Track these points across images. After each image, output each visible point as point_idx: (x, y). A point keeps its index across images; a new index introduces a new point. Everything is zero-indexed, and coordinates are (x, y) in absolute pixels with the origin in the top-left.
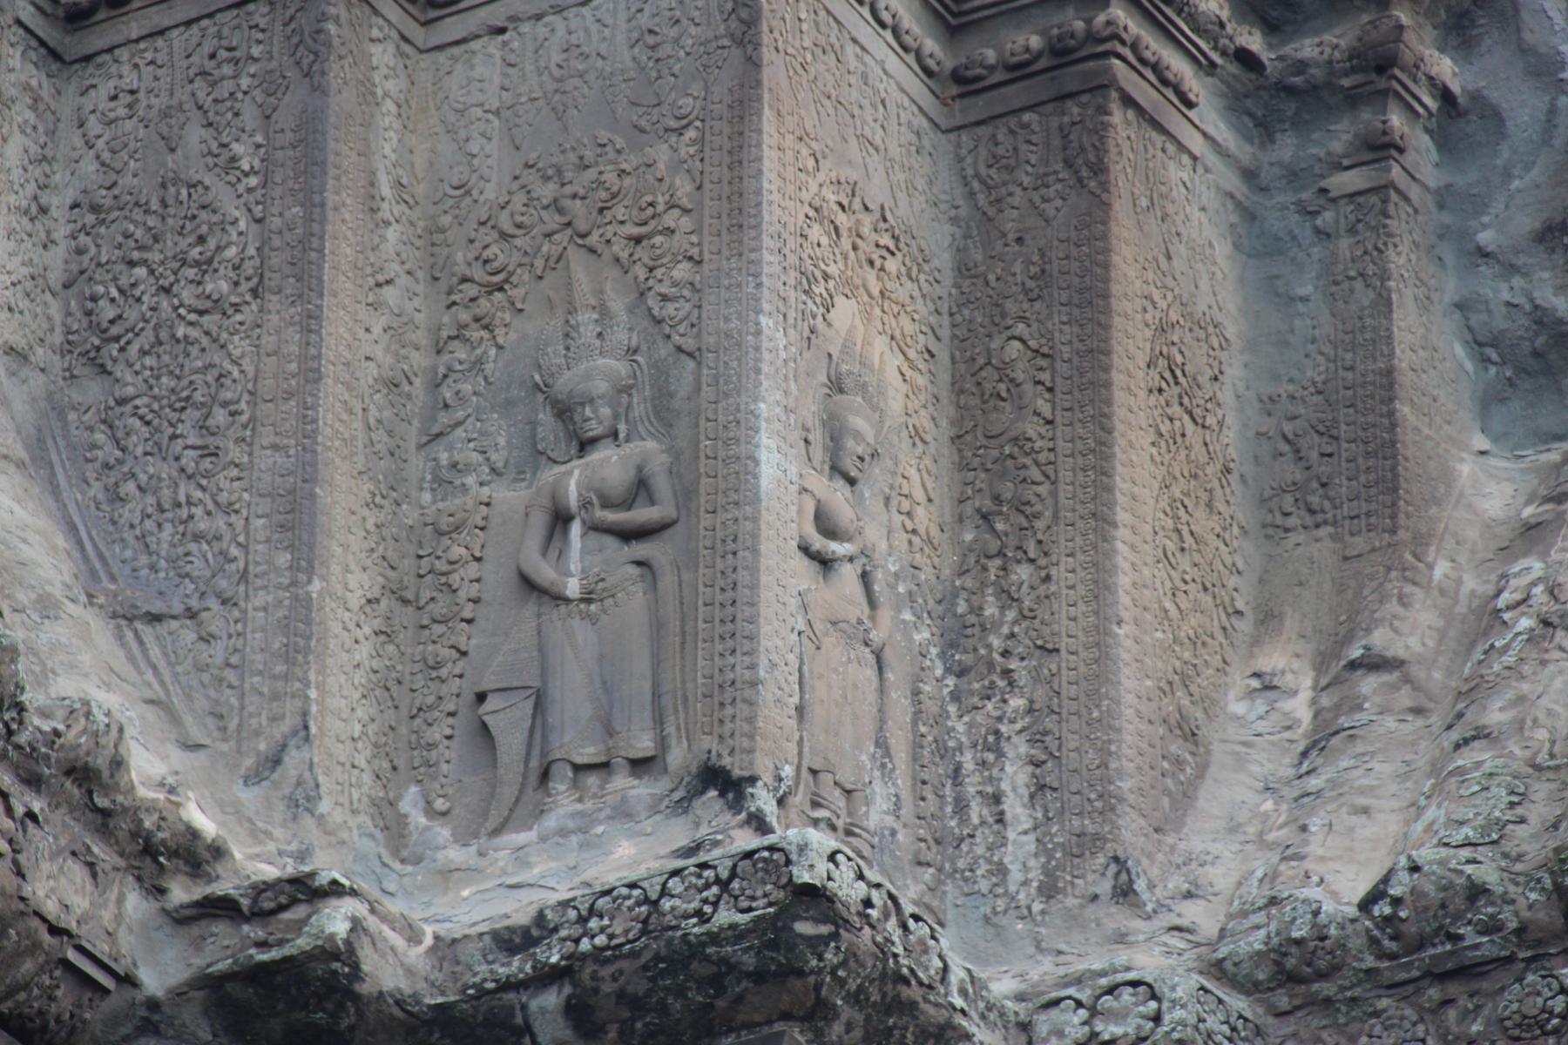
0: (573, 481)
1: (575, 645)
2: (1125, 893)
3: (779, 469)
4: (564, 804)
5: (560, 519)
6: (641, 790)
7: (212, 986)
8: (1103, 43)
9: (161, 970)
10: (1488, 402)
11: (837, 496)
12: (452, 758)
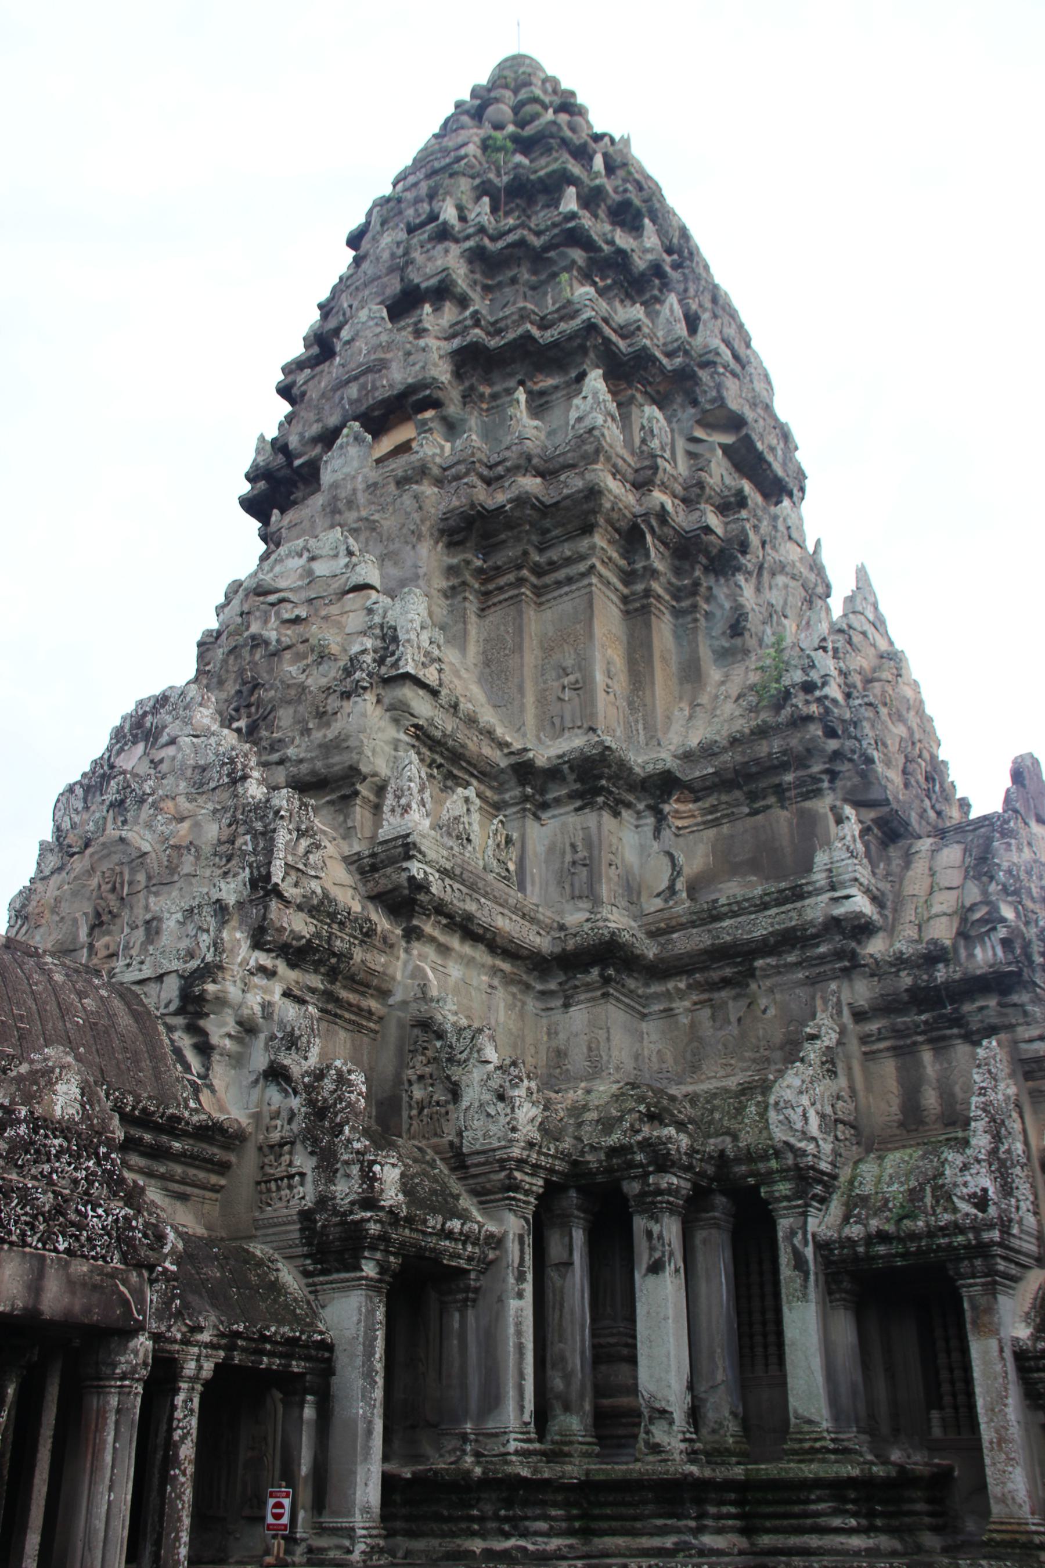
0: (566, 681)
1: (568, 707)
2: (659, 744)
3: (600, 677)
4: (567, 734)
5: (564, 687)
6: (579, 731)
7: (512, 766)
8: (649, 605)
9: (503, 763)
10: (715, 661)
11: (610, 682)
12: (548, 727)
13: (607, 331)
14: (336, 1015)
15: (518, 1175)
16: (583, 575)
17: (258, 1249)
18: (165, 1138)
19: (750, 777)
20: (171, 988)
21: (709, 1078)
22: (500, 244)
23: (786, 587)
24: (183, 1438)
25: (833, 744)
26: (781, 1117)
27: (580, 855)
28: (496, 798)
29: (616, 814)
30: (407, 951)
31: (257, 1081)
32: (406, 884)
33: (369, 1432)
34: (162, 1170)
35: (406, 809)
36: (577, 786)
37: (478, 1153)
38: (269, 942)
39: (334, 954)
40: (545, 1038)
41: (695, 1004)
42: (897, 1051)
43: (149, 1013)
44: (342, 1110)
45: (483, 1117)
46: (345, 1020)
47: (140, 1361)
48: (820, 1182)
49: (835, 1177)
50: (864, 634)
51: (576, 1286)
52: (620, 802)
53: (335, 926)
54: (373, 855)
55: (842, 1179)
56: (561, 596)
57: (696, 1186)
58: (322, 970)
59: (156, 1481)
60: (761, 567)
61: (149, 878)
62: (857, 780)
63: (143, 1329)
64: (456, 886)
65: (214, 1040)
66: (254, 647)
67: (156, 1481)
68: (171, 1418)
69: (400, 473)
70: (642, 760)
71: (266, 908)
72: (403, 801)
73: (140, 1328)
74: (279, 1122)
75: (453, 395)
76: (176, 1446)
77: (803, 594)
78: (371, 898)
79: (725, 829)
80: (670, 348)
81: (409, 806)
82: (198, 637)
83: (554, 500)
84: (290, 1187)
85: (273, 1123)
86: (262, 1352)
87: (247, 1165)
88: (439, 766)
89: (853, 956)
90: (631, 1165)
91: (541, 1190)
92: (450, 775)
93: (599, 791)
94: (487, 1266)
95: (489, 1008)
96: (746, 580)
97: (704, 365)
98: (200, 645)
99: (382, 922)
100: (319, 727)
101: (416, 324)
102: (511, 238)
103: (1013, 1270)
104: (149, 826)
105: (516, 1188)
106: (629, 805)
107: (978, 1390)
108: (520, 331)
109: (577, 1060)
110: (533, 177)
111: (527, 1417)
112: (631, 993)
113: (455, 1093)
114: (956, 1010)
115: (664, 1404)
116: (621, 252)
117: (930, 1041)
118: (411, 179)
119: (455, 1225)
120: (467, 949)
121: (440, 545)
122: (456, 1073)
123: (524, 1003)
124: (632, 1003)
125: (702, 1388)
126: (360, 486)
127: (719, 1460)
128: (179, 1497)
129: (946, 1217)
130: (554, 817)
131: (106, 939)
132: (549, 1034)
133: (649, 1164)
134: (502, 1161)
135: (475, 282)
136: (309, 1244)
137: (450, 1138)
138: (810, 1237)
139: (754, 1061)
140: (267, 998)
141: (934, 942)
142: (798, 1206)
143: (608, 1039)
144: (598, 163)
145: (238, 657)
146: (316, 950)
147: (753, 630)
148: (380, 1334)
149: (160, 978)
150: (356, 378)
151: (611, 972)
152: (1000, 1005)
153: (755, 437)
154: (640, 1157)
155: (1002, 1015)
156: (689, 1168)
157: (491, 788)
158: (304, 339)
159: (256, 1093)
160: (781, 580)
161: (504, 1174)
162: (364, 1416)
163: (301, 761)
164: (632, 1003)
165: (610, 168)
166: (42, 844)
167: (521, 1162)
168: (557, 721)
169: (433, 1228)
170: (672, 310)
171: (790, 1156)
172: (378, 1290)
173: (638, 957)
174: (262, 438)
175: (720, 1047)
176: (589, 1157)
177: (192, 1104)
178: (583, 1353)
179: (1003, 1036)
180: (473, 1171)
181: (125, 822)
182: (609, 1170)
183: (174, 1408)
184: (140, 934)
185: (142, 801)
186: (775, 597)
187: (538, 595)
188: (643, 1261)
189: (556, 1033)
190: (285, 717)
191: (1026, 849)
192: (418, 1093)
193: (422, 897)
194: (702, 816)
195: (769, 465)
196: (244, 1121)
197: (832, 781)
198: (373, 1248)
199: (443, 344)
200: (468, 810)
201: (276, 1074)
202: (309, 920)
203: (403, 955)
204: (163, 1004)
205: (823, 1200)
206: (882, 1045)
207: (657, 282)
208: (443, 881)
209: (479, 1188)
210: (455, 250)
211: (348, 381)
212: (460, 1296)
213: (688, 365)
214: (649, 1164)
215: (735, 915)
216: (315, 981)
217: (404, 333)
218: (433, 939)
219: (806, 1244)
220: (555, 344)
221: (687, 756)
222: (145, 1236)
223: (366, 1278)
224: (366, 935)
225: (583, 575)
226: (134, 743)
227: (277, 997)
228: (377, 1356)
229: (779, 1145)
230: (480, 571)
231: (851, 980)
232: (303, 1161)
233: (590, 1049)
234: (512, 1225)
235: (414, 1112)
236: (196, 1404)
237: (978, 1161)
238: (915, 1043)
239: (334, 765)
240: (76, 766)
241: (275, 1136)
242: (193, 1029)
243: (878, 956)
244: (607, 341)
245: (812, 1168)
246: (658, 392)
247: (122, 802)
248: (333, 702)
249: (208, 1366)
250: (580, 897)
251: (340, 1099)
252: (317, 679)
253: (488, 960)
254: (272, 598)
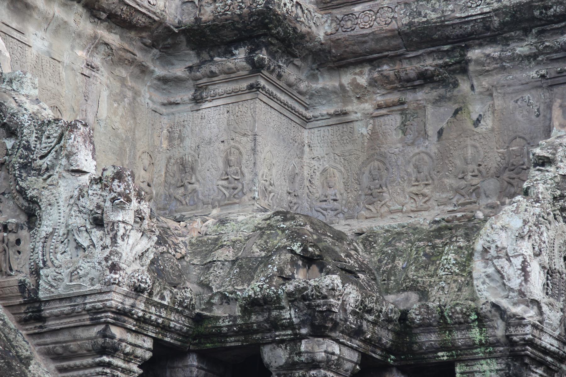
15: (116, 331)
21: (391, 212)
26: (491, 270)
37: (61, 299)
40: (165, 145)
41: (380, 107)
45: (71, 249)
48: (540, 363)
57: (365, 358)
90: (276, 324)
95: (86, 97)
105: (111, 349)
109: (209, 177)
112: (289, 88)
113: (32, 214)
122: (33, 184)
123: (137, 94)
124: (291, 102)
132: (170, 139)
133: (303, 323)
137: (21, 277)
139: (457, 191)
143: (254, 150)
151: (263, 55)
154: (289, 314)
156: (358, 333)
161: (96, 330)
164: (291, 102)
167: (122, 314)
171: (500, 325)
173: (303, 36)
175: (410, 169)
176: (218, 312)
180: (52, 324)
182: (246, 331)
189: (181, 139)
209: (59, 350)
214: (303, 323)
233: (228, 163)
245: (530, 343)
253: (87, 27)
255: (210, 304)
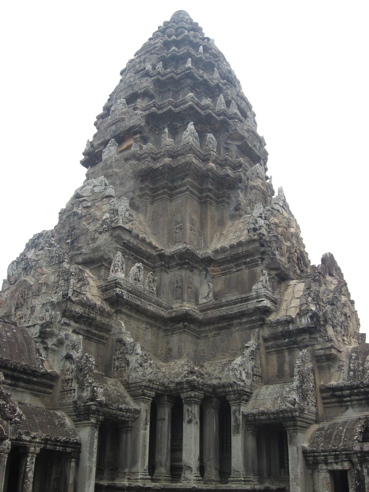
0: (178, 226)
1: (178, 235)
3: (188, 225)
4: (177, 244)
5: (177, 228)
10: (230, 219)
13: (197, 108)
14: (91, 338)
15: (145, 391)
16: (185, 191)
17: (59, 413)
18: (31, 377)
19: (237, 259)
20: (38, 328)
22: (165, 78)
23: (256, 193)
24: (30, 470)
25: (262, 249)
26: (233, 374)
27: (179, 284)
28: (152, 265)
29: (192, 271)
30: (116, 317)
31: (63, 359)
32: (115, 295)
33: (91, 471)
34: (31, 387)
35: (117, 271)
36: (179, 262)
37: (133, 383)
38: (68, 315)
39: (90, 319)
40: (166, 345)
41: (215, 334)
42: (278, 352)
43: (29, 337)
44: (87, 369)
46: (94, 339)
47: (6, 447)
48: (246, 395)
49: (252, 393)
50: (278, 211)
51: (165, 427)
52: (193, 267)
53: (91, 309)
54: (106, 286)
55: (254, 394)
56: (178, 197)
58: (87, 323)
59: (21, 483)
60: (246, 188)
61: (33, 293)
62: (270, 261)
63: (8, 438)
64: (133, 296)
65: (49, 346)
66: (74, 216)
67: (21, 483)
68: (26, 465)
69: (126, 156)
70: (200, 253)
71: (67, 304)
72: (116, 268)
73: (6, 438)
74: (69, 373)
75: (147, 129)
76: (27, 473)
77: (262, 195)
78: (105, 300)
79: (228, 276)
80: (219, 113)
81: (117, 270)
82: (59, 211)
83: (176, 166)
84: (71, 393)
85: (67, 373)
86: (57, 445)
87: (59, 386)
88: (132, 256)
89: (264, 320)
91: (154, 396)
92: (136, 258)
93: (185, 263)
94: (135, 420)
96: (241, 192)
97: (231, 118)
98: (60, 213)
99: (107, 308)
100: (93, 243)
101: (134, 106)
102: (168, 76)
103: (304, 425)
104: (33, 276)
105: (144, 395)
106: (196, 268)
107: (290, 463)
108: (168, 108)
109: (175, 352)
110: (178, 55)
111: (145, 468)
112: (194, 331)
113: (128, 363)
114: (295, 339)
115: (189, 465)
116: (205, 81)
117: (288, 349)
118: (140, 54)
119: (123, 406)
120: (138, 316)
121: (139, 180)
122: (128, 356)
123: (158, 333)
124: (194, 334)
125: (205, 460)
126: (114, 161)
127: (209, 483)
128: (28, 488)
129: (284, 407)
130: (172, 271)
131: (20, 312)
132: (167, 343)
133: (189, 388)
134: (140, 386)
135: (156, 90)
136: (75, 412)
137: (126, 378)
138: (241, 413)
140: (67, 332)
141: (290, 316)
142: (238, 403)
144: (201, 48)
145: (70, 219)
146: (84, 317)
147: (243, 208)
148: (96, 441)
149: (34, 326)
150: (114, 124)
152: (310, 338)
153: (248, 142)
155: (309, 341)
156: (202, 389)
157: (151, 262)
158: (103, 108)
159: (62, 363)
160: (254, 191)
161: (141, 391)
162: (89, 466)
163: (86, 254)
164: (194, 334)
165: (206, 49)
166: (4, 280)
167: (146, 387)
168: (174, 239)
169: (115, 407)
170: (221, 100)
172: (95, 427)
173: (196, 319)
174: (88, 141)
177: (41, 367)
178: (168, 447)
179: (310, 348)
180: (132, 389)
181: (26, 275)
182: (176, 390)
183: (27, 461)
184: (29, 312)
185: (31, 268)
186: (250, 197)
187: (171, 197)
188: (186, 419)
189: (169, 343)
190: (82, 239)
191: (323, 285)
192: (117, 363)
193: (120, 299)
194: (221, 271)
195: (254, 151)
196: (58, 372)
197: (262, 261)
198: (94, 413)
199: (143, 112)
200: (139, 271)
201: (69, 357)
202: (81, 308)
203: (115, 318)
204: (34, 334)
205: (247, 401)
206: (272, 350)
207: (218, 90)
208: (128, 294)
209: (133, 395)
210: (150, 80)
211: (112, 125)
212: (126, 429)
213: (225, 119)
214: (189, 388)
215: (227, 305)
216: (84, 327)
217: (130, 109)
218: (125, 314)
219: (240, 415)
220: (180, 112)
221: (216, 252)
222: (10, 410)
223: (91, 423)
224: (102, 312)
225: (185, 191)
226: (32, 249)
227: (70, 332)
228: (95, 447)
229: (232, 383)
230: (152, 189)
231: (263, 328)
232: (75, 385)
233: (179, 349)
234: (144, 408)
235: (115, 369)
236: (34, 460)
237: (294, 390)
238: (283, 349)
239: (96, 256)
240: (15, 255)
241: (68, 377)
242: (43, 342)
243: (272, 320)
244: (197, 112)
245: (242, 390)
246: (215, 128)
247: (26, 268)
248: (97, 235)
249: (38, 449)
250: (178, 298)
251: (86, 366)
252: (92, 228)
253: (145, 319)
254: (81, 199)
255: (169, 384)
